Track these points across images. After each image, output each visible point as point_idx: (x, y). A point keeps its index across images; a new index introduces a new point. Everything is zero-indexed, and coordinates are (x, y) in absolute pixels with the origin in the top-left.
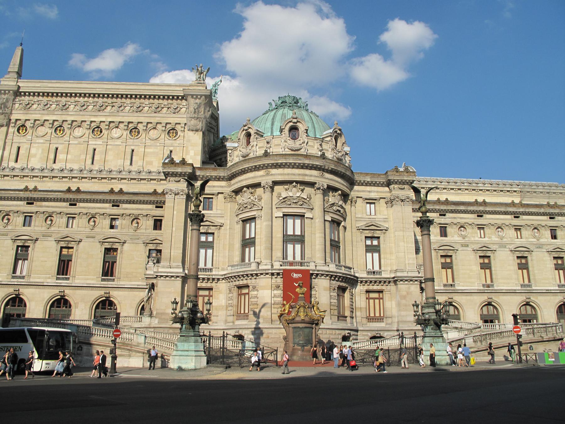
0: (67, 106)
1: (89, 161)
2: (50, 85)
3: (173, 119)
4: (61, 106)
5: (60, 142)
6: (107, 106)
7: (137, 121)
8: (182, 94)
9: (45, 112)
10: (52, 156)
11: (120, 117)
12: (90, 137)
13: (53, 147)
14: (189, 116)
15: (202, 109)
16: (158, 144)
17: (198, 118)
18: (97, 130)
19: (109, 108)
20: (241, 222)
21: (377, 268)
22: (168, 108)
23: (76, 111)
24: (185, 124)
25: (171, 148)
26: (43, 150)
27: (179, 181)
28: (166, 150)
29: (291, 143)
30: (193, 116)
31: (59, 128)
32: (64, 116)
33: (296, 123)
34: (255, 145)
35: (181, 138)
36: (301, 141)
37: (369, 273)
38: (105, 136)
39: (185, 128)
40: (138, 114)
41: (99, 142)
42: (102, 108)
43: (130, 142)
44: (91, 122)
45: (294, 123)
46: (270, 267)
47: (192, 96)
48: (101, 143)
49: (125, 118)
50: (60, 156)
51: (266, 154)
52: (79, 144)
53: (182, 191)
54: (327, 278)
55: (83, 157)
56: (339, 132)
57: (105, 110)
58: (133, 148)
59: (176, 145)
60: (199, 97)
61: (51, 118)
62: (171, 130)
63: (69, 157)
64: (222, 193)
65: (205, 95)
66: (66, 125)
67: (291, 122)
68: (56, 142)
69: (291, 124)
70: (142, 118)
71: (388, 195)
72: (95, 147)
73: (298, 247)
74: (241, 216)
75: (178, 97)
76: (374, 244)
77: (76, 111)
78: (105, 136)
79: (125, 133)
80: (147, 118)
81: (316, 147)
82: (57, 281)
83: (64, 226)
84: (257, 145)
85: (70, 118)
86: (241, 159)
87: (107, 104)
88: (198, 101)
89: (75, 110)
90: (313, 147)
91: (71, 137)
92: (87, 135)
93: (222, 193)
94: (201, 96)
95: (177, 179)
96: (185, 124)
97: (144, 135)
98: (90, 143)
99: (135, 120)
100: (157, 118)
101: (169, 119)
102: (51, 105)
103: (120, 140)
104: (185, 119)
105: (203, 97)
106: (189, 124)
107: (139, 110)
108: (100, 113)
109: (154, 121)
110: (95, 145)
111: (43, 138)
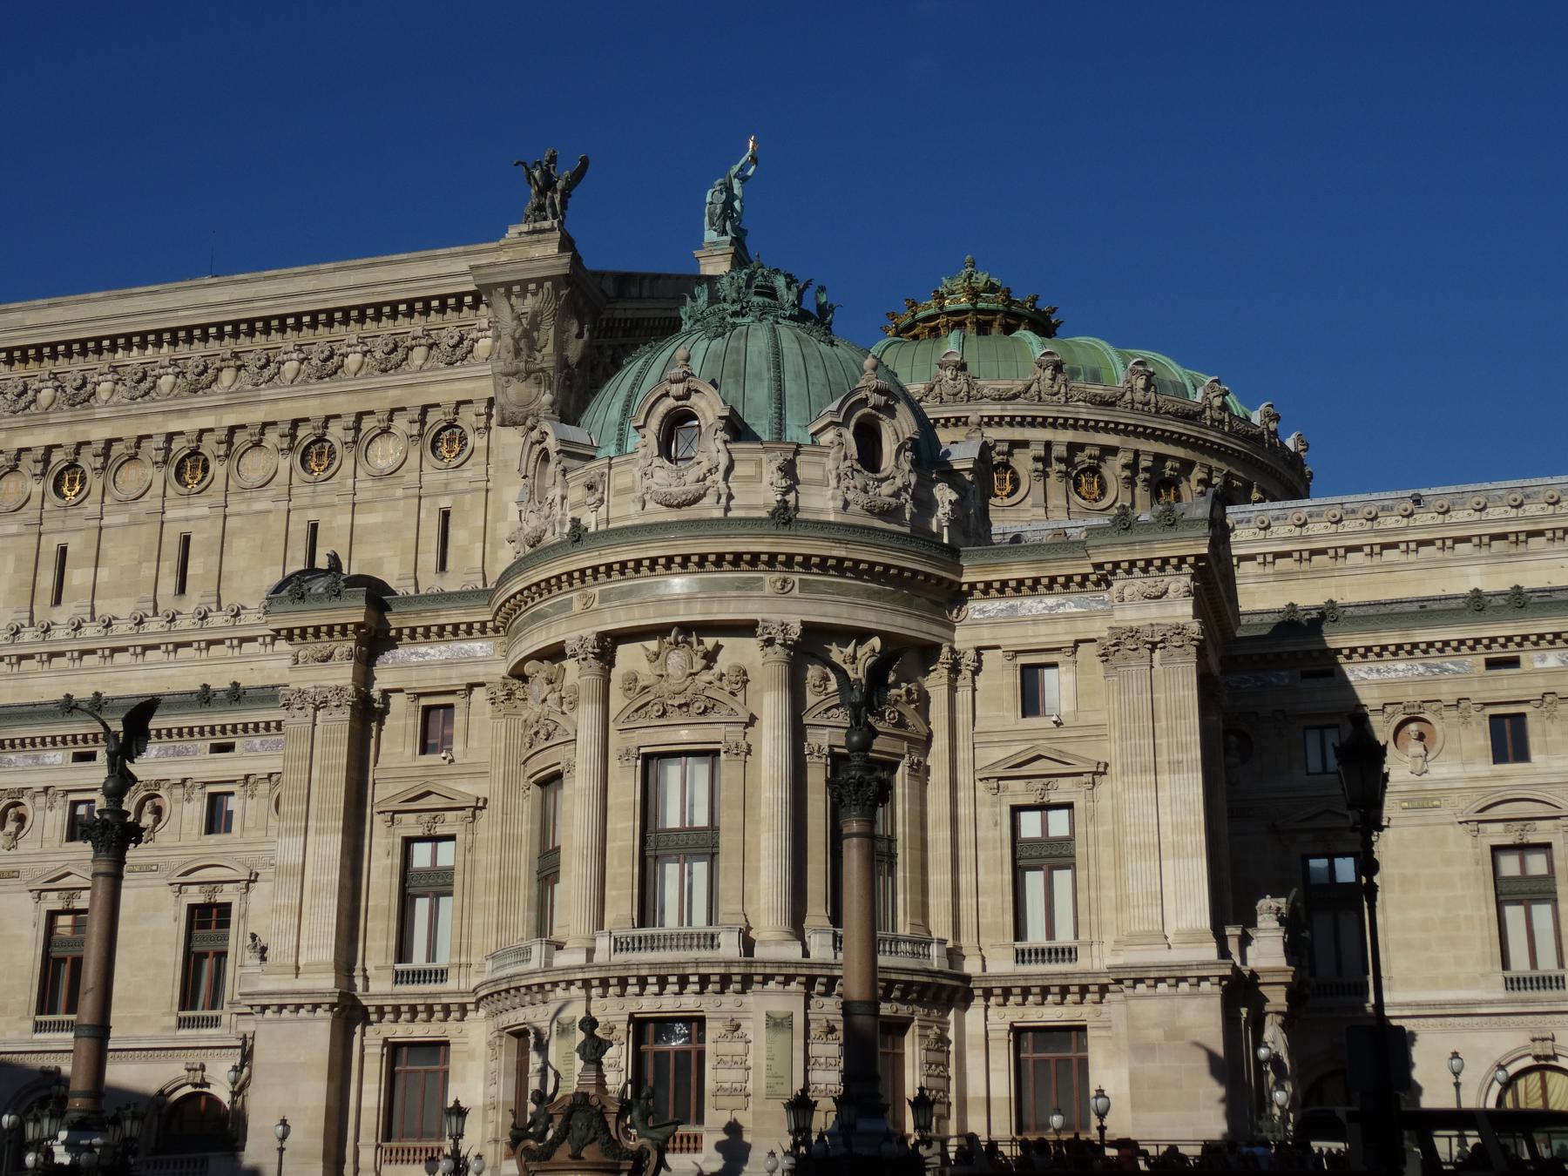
0: (89, 387)
1: (169, 584)
2: (31, 318)
3: (445, 394)
4: (68, 390)
5: (73, 523)
6: (220, 370)
7: (323, 414)
8: (472, 288)
9: (20, 420)
10: (47, 580)
11: (265, 407)
12: (170, 492)
13: (50, 545)
14: (500, 366)
15: (547, 334)
16: (399, 492)
17: (529, 374)
18: (189, 465)
19: (227, 376)
20: (536, 791)
21: (1064, 937)
22: (430, 347)
23: (115, 405)
24: (491, 402)
25: (445, 502)
26: (18, 559)
27: (328, 658)
28: (429, 511)
29: (664, 477)
30: (513, 368)
31: (64, 475)
32: (80, 428)
33: (686, 396)
34: (558, 500)
35: (479, 457)
36: (705, 466)
37: (1021, 956)
38: (219, 484)
39: (489, 416)
40: (327, 385)
41: (200, 508)
42: (202, 380)
43: (302, 493)
44: (170, 437)
45: (678, 398)
46: (580, 959)
47: (508, 286)
48: (206, 511)
49: (282, 405)
50: (77, 577)
51: (578, 534)
52: (131, 524)
53: (339, 690)
54: (793, 986)
55: (148, 570)
56: (875, 399)
57: (214, 387)
58: (312, 516)
59: (460, 486)
60: (532, 287)
61: (38, 439)
62: (444, 429)
63: (103, 574)
64: (482, 685)
65: (553, 279)
66: (87, 461)
67: (667, 395)
68: (60, 525)
69: (669, 403)
70: (340, 399)
71: (1099, 628)
72: (185, 528)
73: (700, 868)
74: (533, 766)
75: (460, 297)
76: (1053, 833)
77: (115, 405)
78: (219, 484)
79: (284, 463)
80: (355, 397)
81: (766, 479)
82: (38, 1036)
83: (58, 834)
84: (563, 498)
85: (99, 433)
86: (528, 550)
87: (218, 364)
88: (529, 304)
89: (115, 399)
90: (758, 478)
91: (107, 499)
92: (157, 489)
93: (482, 685)
94: (539, 282)
95: (324, 646)
96: (491, 402)
97: (348, 465)
98: (170, 514)
99: (313, 408)
100: (392, 393)
101: (433, 389)
102: (38, 391)
103: (272, 490)
104: (490, 382)
105: (548, 285)
106: (500, 400)
107: (330, 367)
108: (199, 401)
109: (381, 403)
110: (187, 519)
111: (20, 516)
